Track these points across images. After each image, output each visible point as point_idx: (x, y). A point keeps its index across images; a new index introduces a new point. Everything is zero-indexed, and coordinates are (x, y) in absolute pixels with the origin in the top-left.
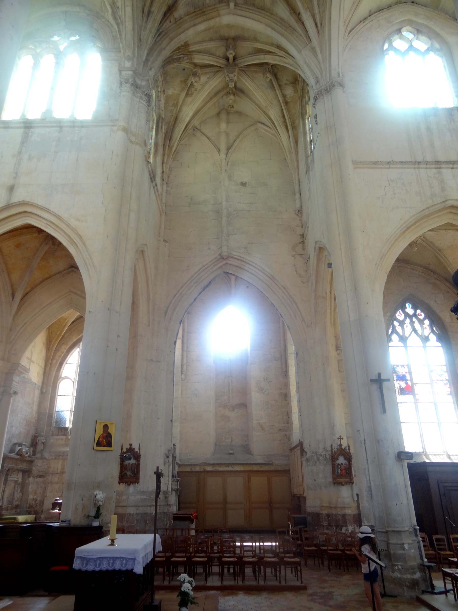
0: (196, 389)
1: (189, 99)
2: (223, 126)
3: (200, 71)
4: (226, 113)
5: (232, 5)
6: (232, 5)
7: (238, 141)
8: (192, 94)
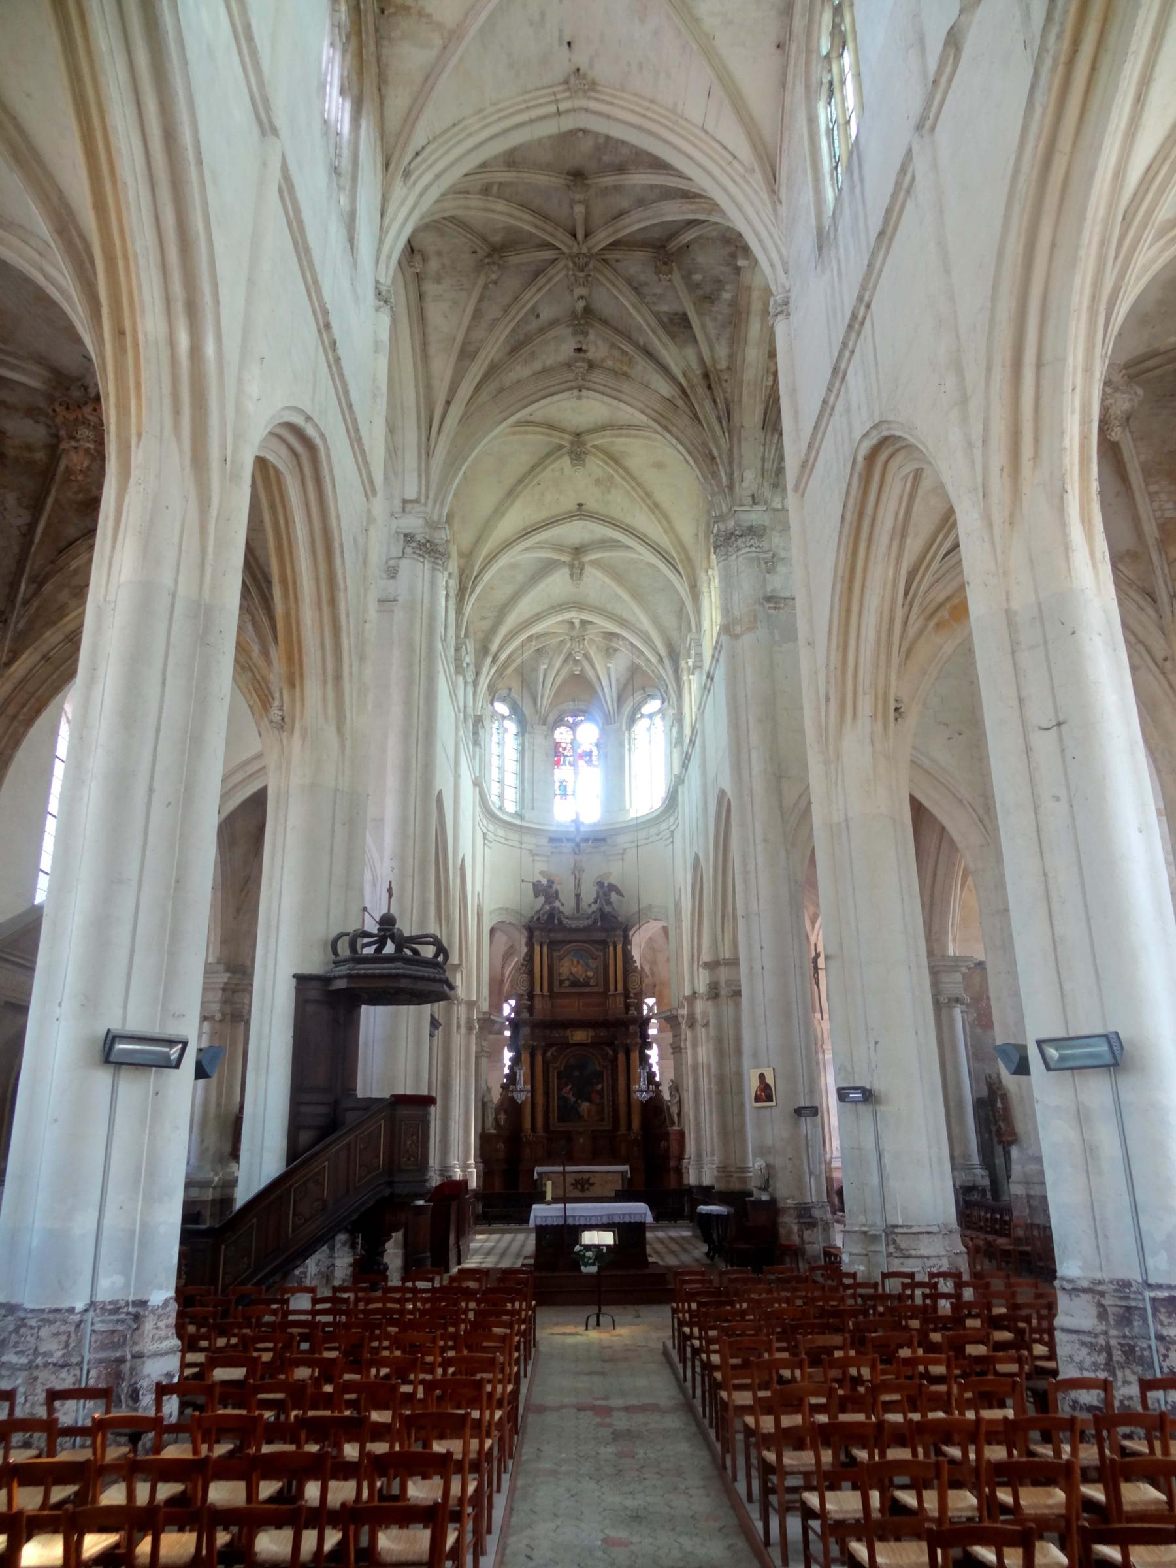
5: (741, 263)
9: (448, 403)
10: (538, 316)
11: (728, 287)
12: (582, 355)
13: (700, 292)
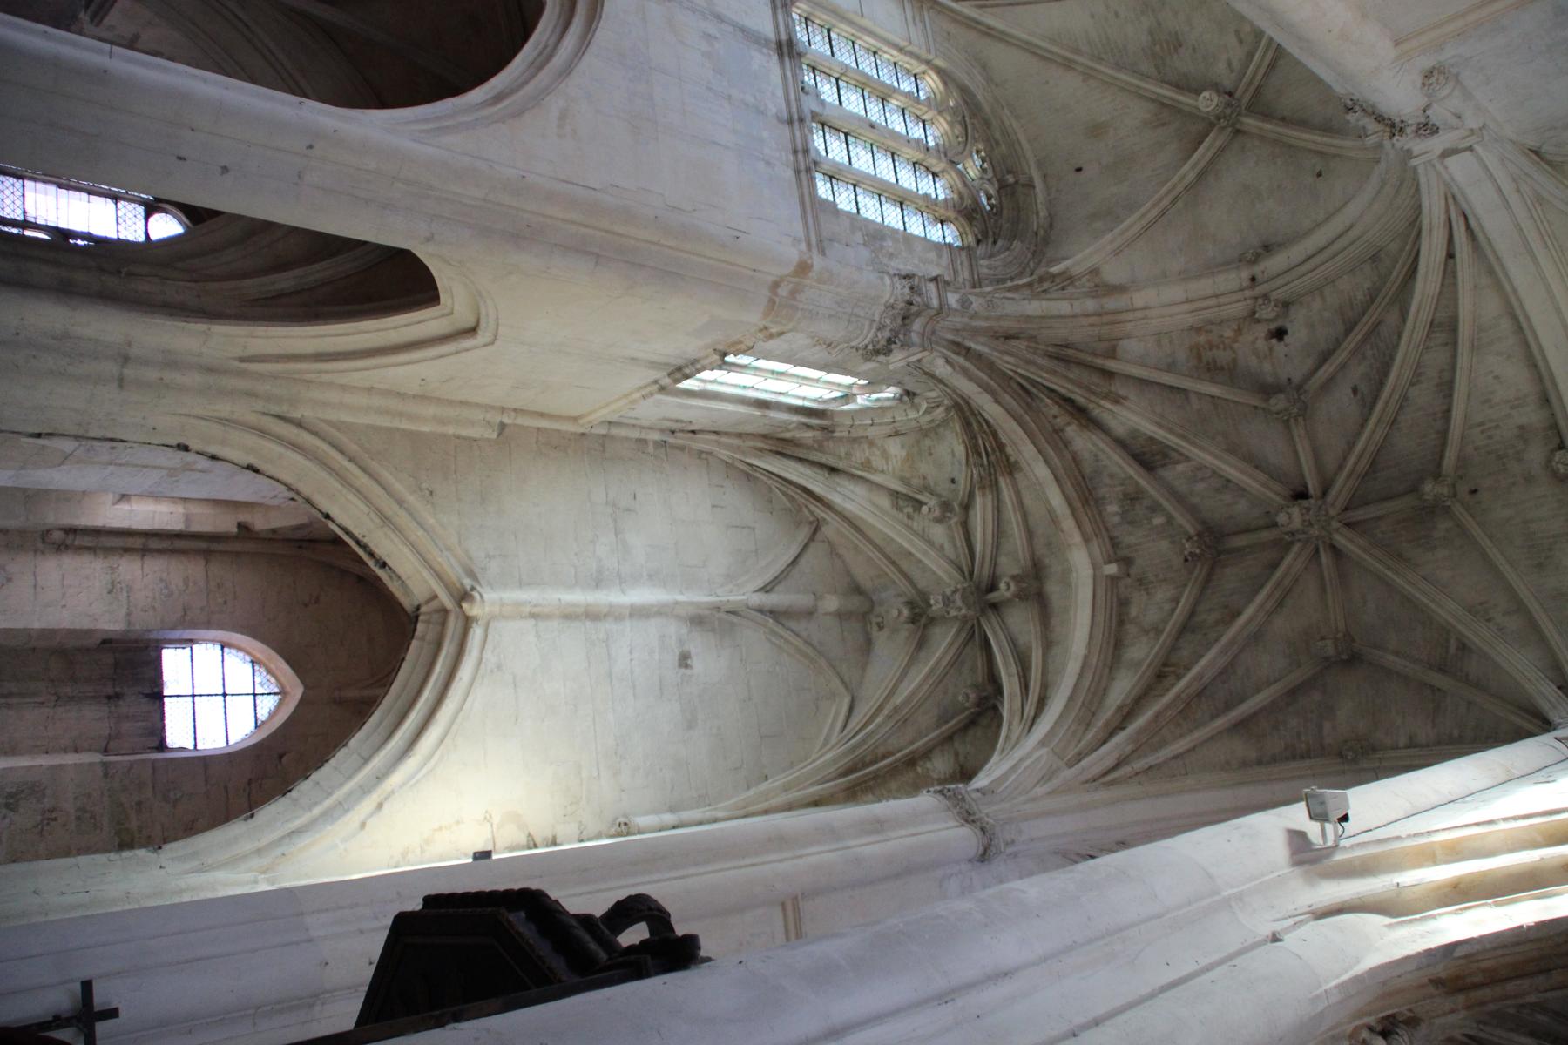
0: (9, 580)
1: (885, 502)
2: (832, 603)
3: (955, 519)
4: (862, 612)
6: (1112, 569)
7: (798, 642)
8: (899, 509)
9: (1451, 255)
10: (1355, 391)
11: (1116, 519)
12: (1273, 326)
13: (1146, 502)
